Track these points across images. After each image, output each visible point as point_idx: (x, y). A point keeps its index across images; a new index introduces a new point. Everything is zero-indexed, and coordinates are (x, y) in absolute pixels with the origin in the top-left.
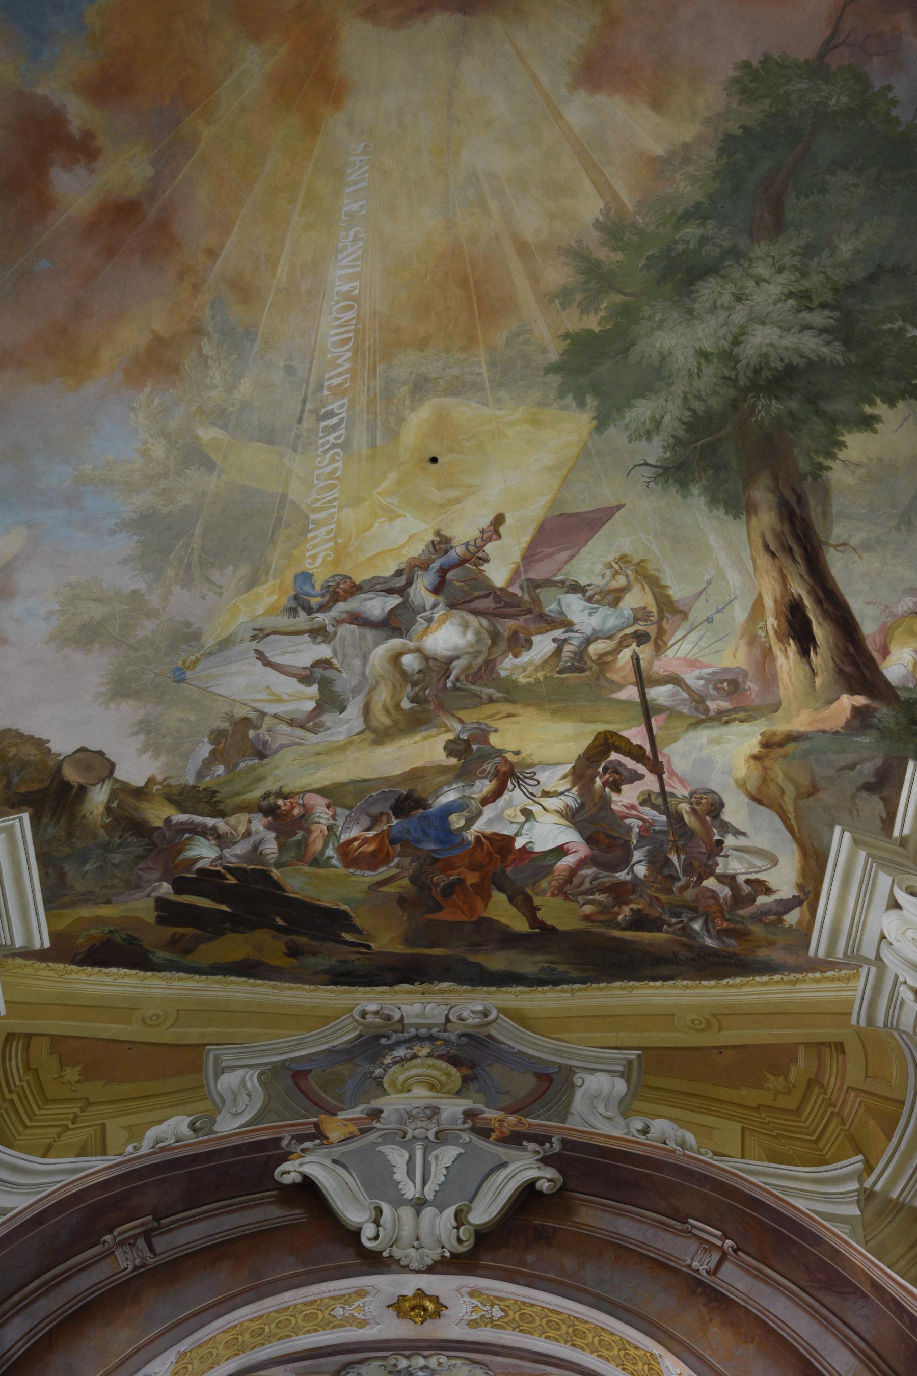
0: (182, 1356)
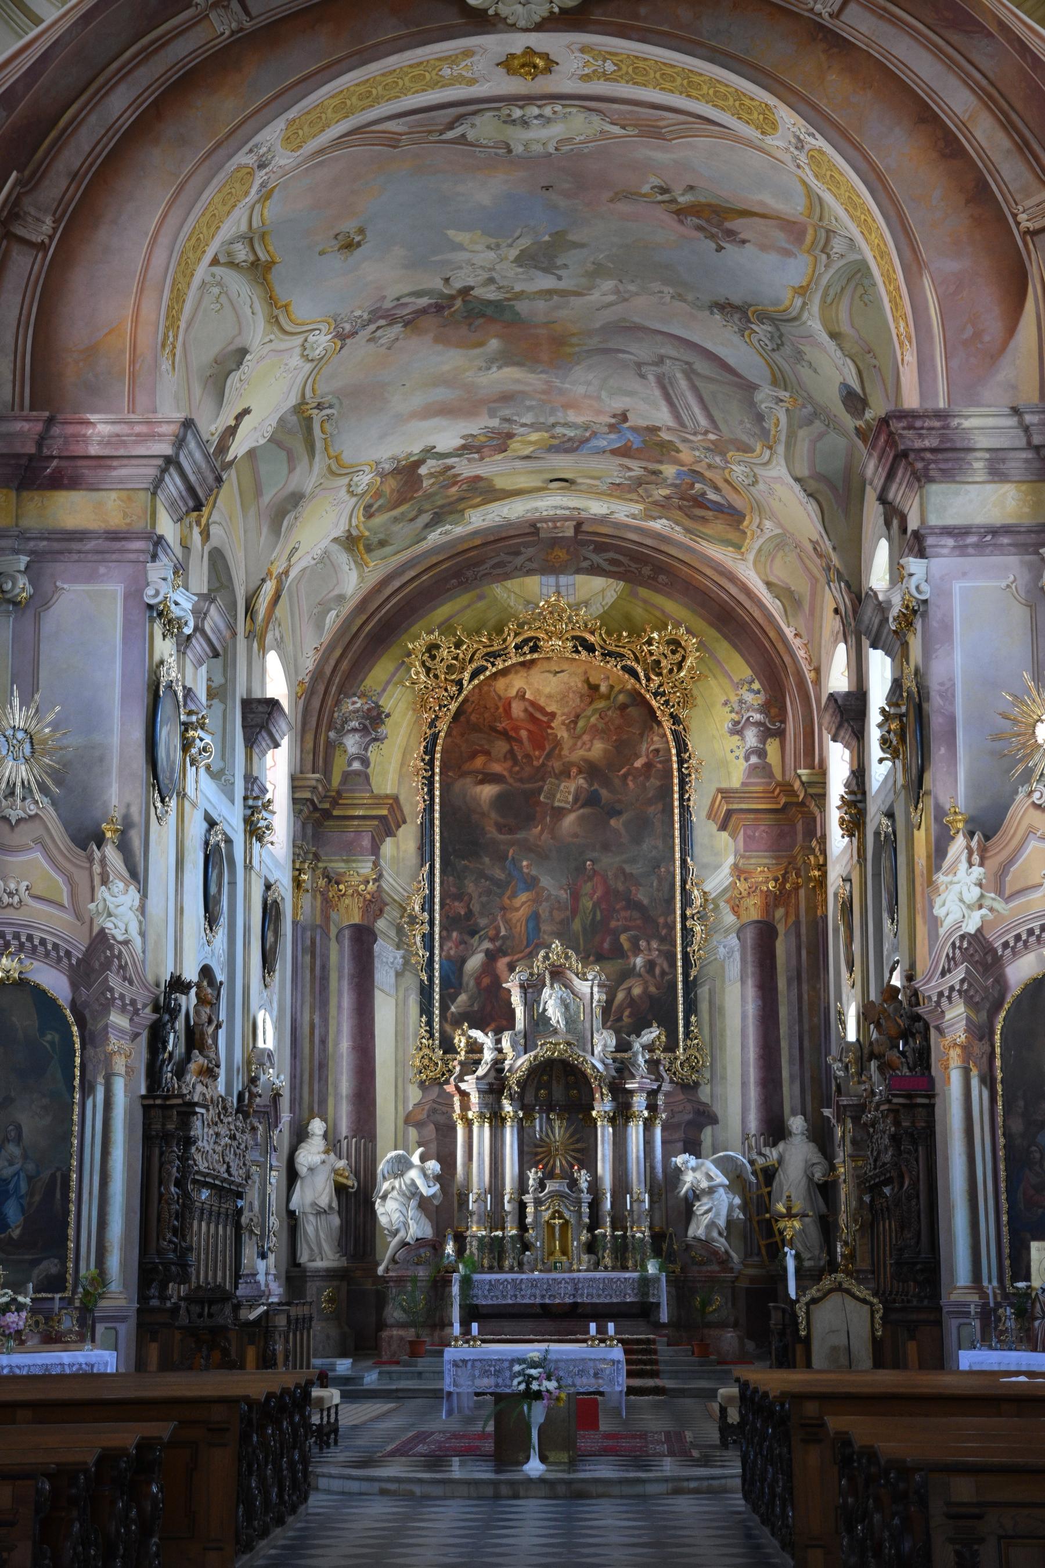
0: (291, 123)
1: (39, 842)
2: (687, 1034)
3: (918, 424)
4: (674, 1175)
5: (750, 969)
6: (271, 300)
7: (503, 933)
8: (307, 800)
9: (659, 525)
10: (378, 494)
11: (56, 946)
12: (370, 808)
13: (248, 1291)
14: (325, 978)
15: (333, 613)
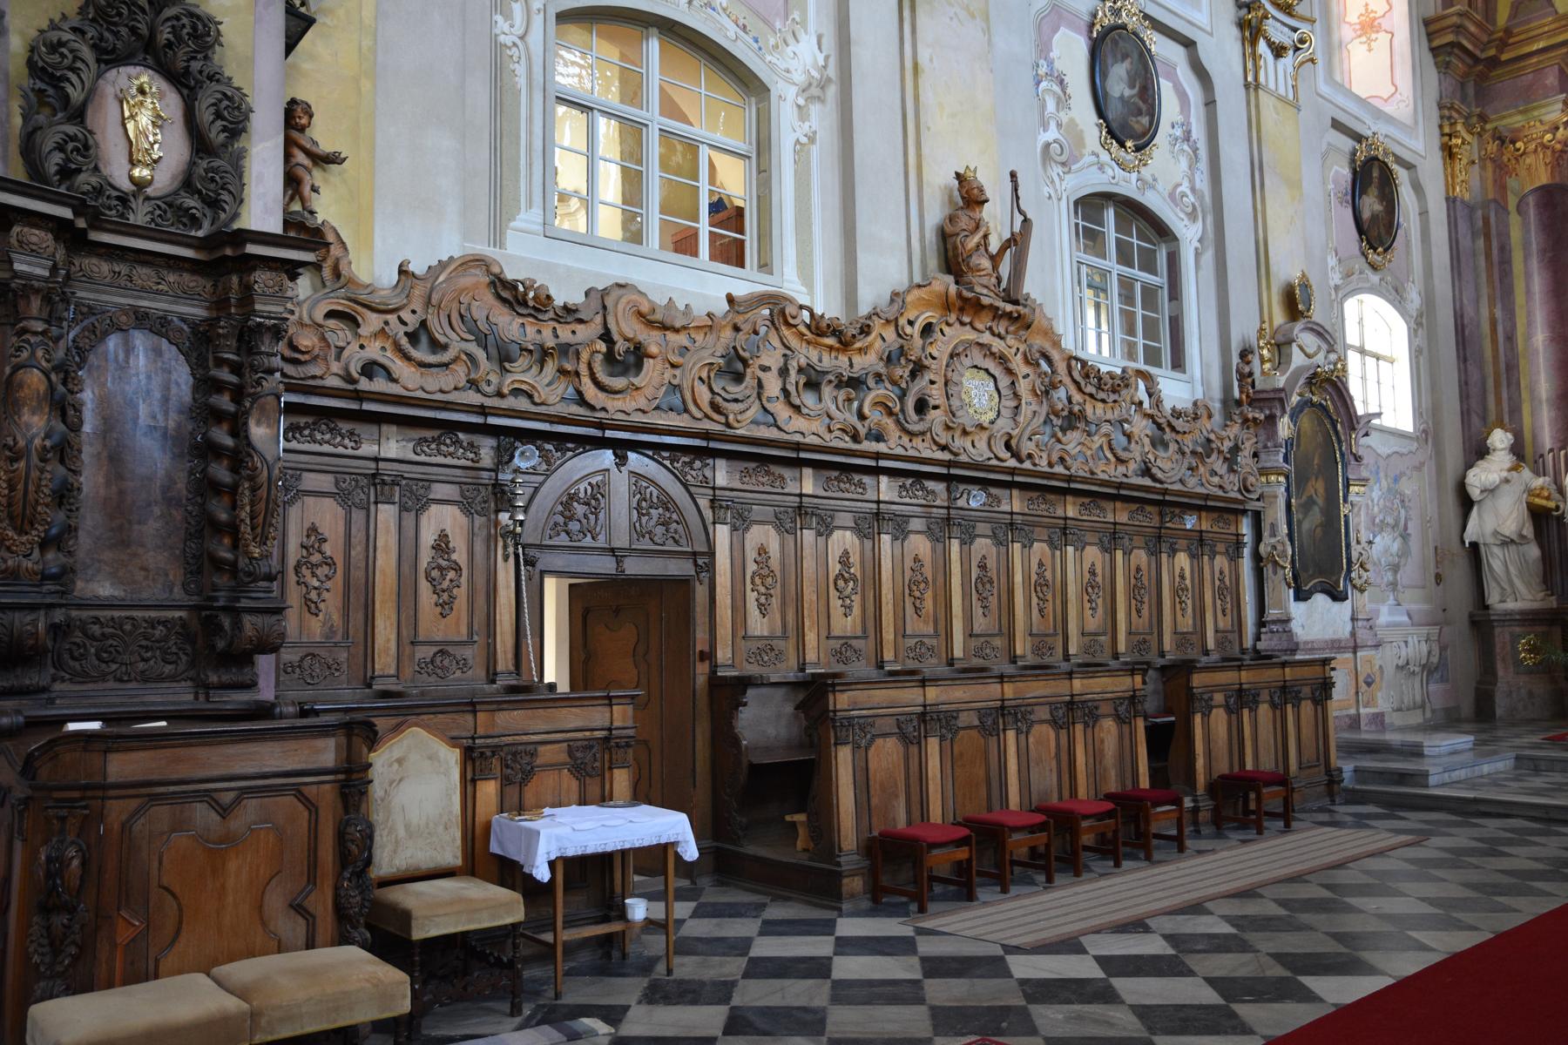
8: (1452, 44)
12: (1555, 35)
13: (1273, 643)
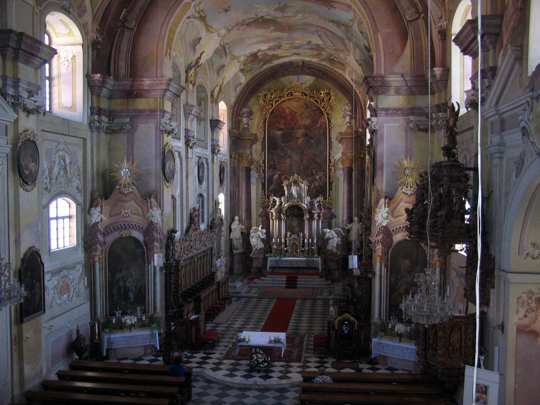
1: (133, 199)
2: (329, 196)
3: (375, 79)
4: (324, 234)
5: (346, 179)
6: (206, 25)
7: (283, 169)
9: (324, 63)
10: (247, 61)
11: (139, 226)
14: (238, 180)
15: (239, 88)
